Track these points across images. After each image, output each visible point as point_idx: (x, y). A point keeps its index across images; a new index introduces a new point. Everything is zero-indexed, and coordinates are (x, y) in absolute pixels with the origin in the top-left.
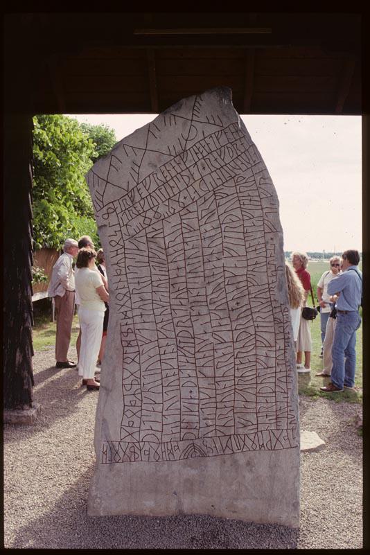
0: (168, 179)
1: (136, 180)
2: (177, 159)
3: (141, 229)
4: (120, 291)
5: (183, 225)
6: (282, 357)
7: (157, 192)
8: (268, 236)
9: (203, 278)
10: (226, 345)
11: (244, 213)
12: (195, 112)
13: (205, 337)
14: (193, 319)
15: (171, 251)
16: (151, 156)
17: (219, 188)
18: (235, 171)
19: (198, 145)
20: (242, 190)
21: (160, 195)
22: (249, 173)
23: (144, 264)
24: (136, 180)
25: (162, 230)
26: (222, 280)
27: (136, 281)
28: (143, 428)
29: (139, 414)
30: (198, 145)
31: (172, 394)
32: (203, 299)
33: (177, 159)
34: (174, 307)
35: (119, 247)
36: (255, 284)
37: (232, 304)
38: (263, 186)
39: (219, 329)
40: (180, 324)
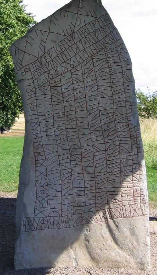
0: (63, 50)
1: (43, 50)
2: (69, 38)
3: (46, 81)
4: (33, 121)
5: (73, 79)
6: (136, 159)
7: (57, 58)
8: (126, 84)
9: (86, 111)
10: (101, 153)
11: (111, 71)
12: (79, 9)
13: (88, 148)
14: (80, 137)
15: (66, 94)
16: (52, 36)
17: (95, 55)
18: (105, 44)
19: (81, 29)
20: (110, 56)
21: (59, 61)
22: (113, 46)
23: (48, 103)
24: (43, 50)
25: (60, 82)
26: (97, 112)
27: (44, 114)
28: (49, 208)
29: (46, 199)
30: (81, 29)
31: (67, 186)
32: (86, 124)
33: (69, 38)
34: (68, 130)
35: (32, 93)
36: (119, 114)
37: (105, 127)
38: (122, 54)
39: (97, 142)
40: (72, 140)
